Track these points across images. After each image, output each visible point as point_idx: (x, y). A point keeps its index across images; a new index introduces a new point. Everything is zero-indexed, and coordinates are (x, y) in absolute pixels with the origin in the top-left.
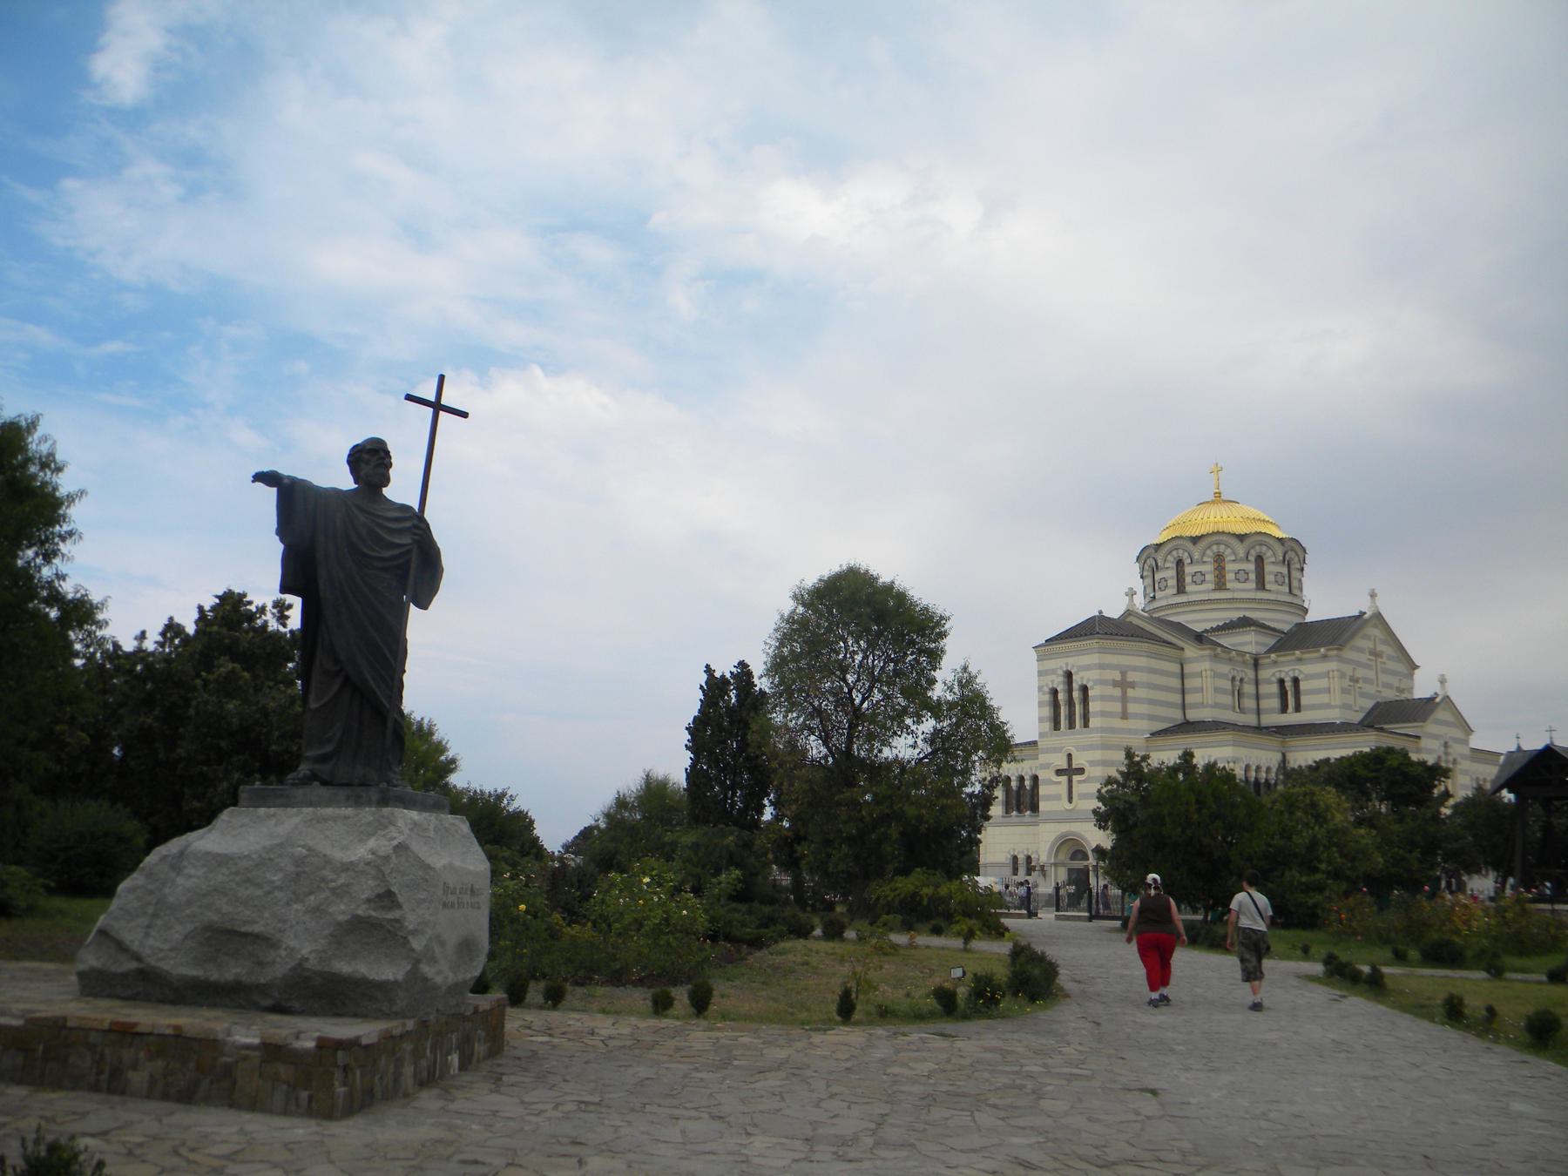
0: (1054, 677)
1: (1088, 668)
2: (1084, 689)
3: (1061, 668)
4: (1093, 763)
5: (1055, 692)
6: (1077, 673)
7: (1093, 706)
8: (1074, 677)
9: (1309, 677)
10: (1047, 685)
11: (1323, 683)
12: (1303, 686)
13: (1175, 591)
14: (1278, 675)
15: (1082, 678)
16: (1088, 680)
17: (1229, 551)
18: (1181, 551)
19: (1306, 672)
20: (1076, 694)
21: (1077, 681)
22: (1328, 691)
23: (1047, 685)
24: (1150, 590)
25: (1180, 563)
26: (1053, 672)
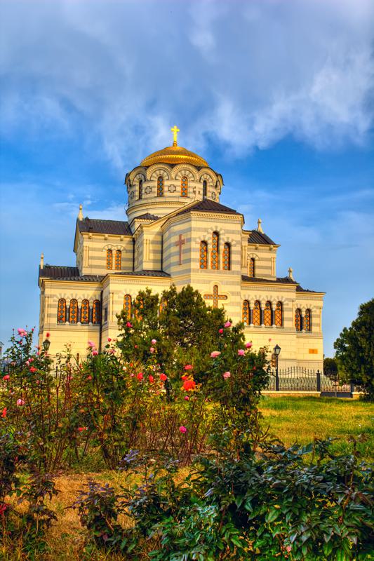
0: (205, 234)
1: (233, 232)
2: (228, 245)
3: (211, 229)
4: (233, 293)
5: (204, 243)
6: (224, 234)
7: (234, 257)
8: (221, 237)
9: (259, 260)
10: (199, 238)
11: (268, 264)
12: (257, 263)
13: (180, 194)
14: (251, 256)
15: (228, 238)
16: (233, 240)
17: (210, 180)
18: (187, 172)
19: (260, 256)
20: (222, 247)
21: (224, 238)
22: (270, 268)
23: (199, 238)
24: (155, 190)
25: (185, 177)
26: (206, 230)
